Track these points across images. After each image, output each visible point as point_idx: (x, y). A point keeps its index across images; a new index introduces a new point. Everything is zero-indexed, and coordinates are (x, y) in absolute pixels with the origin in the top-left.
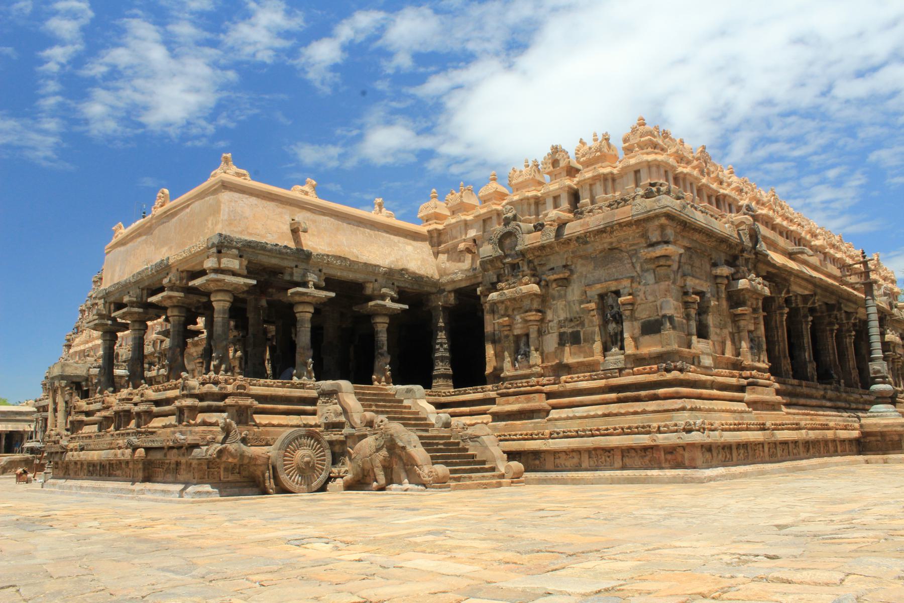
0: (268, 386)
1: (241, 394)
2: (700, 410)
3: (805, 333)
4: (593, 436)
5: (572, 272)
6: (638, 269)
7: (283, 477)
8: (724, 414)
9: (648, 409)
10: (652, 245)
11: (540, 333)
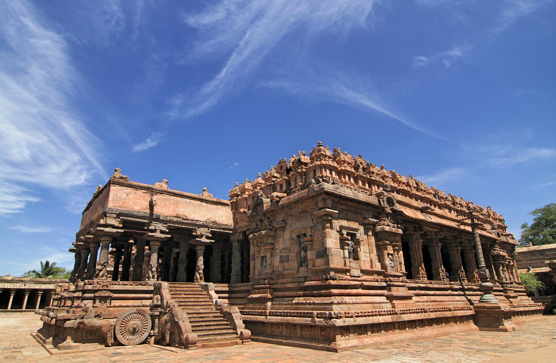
0: (125, 285)
1: (104, 290)
2: (346, 303)
3: (437, 253)
4: (287, 316)
5: (286, 224)
6: (315, 222)
7: (119, 337)
8: (364, 305)
9: (316, 302)
10: (320, 209)
11: (272, 255)
